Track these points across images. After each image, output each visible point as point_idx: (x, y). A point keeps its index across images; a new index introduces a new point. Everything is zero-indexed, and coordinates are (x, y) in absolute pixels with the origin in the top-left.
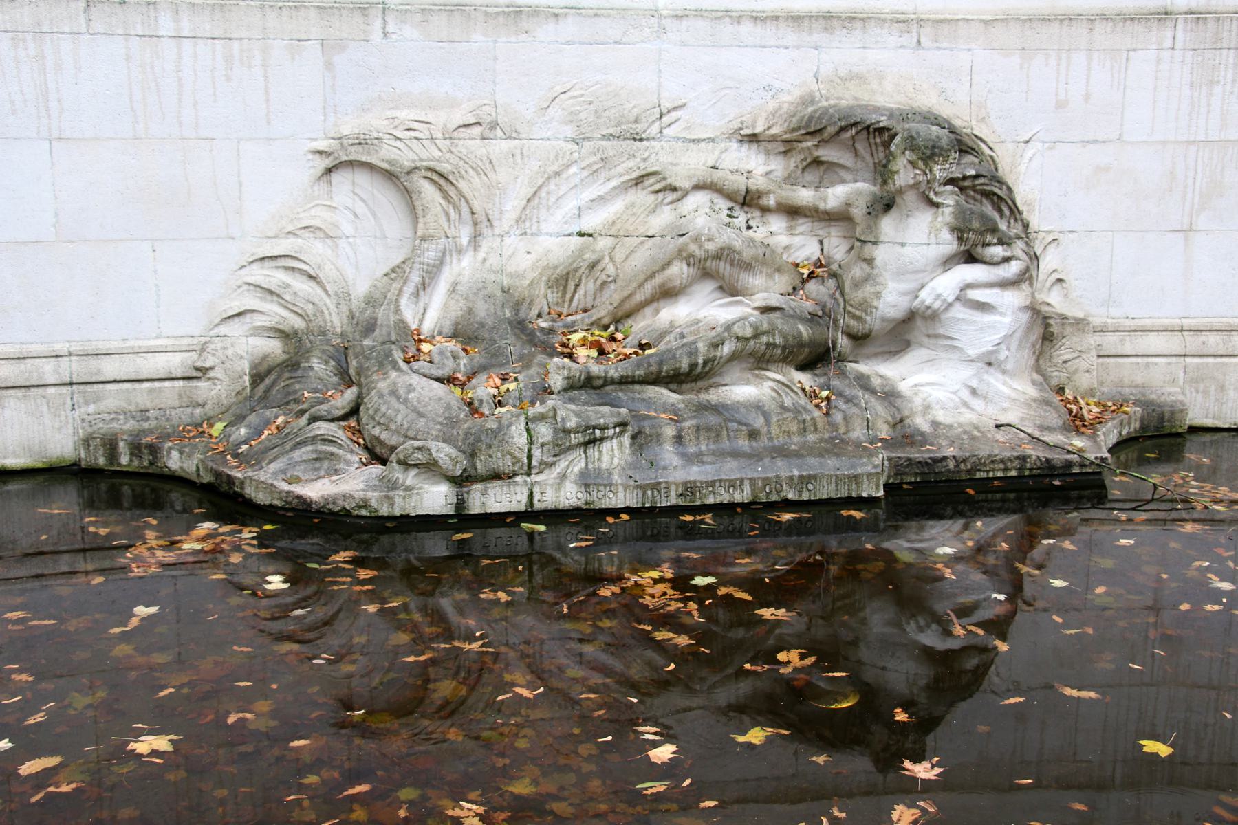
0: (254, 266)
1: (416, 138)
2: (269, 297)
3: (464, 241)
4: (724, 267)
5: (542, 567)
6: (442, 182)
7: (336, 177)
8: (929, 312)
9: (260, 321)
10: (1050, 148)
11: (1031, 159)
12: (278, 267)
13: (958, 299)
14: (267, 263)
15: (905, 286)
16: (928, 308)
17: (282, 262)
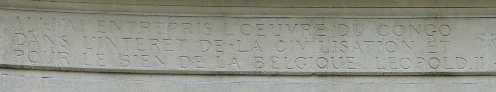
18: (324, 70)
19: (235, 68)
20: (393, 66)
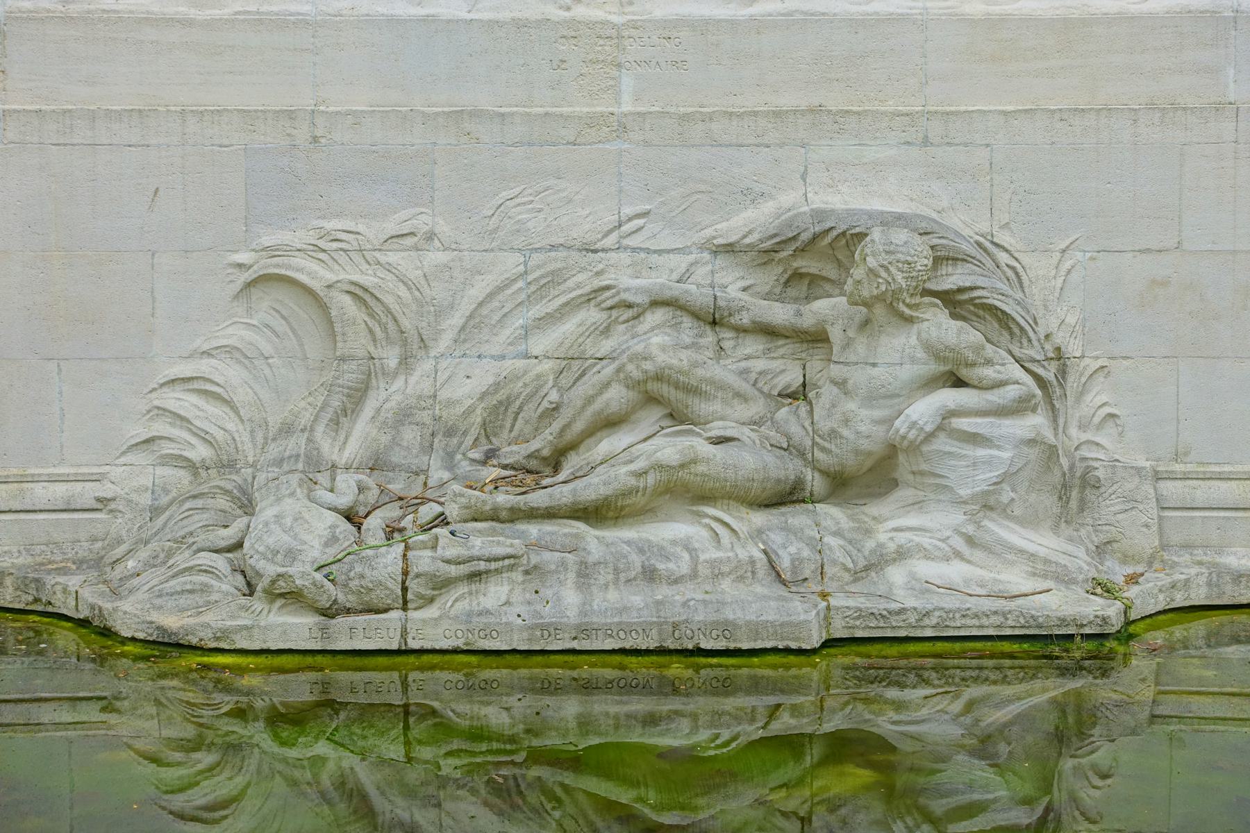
0: (165, 389)
1: (345, 251)
2: (178, 423)
3: (393, 363)
4: (666, 390)
5: (422, 717)
6: (367, 297)
7: (256, 293)
8: (906, 443)
9: (168, 449)
10: (1092, 259)
11: (1069, 271)
12: (189, 390)
13: (940, 428)
14: (178, 387)
15: (878, 414)
16: (904, 438)
17: (196, 385)
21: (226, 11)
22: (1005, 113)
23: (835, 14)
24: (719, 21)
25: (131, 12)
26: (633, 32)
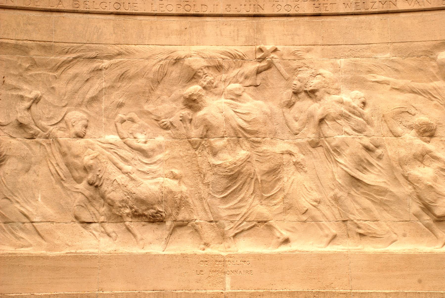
18: (118, 11)
19: (60, 7)
20: (162, 9)
21: (63, 252)
22: (386, 294)
23: (312, 252)
24: (266, 254)
25: (21, 254)
26: (231, 259)
